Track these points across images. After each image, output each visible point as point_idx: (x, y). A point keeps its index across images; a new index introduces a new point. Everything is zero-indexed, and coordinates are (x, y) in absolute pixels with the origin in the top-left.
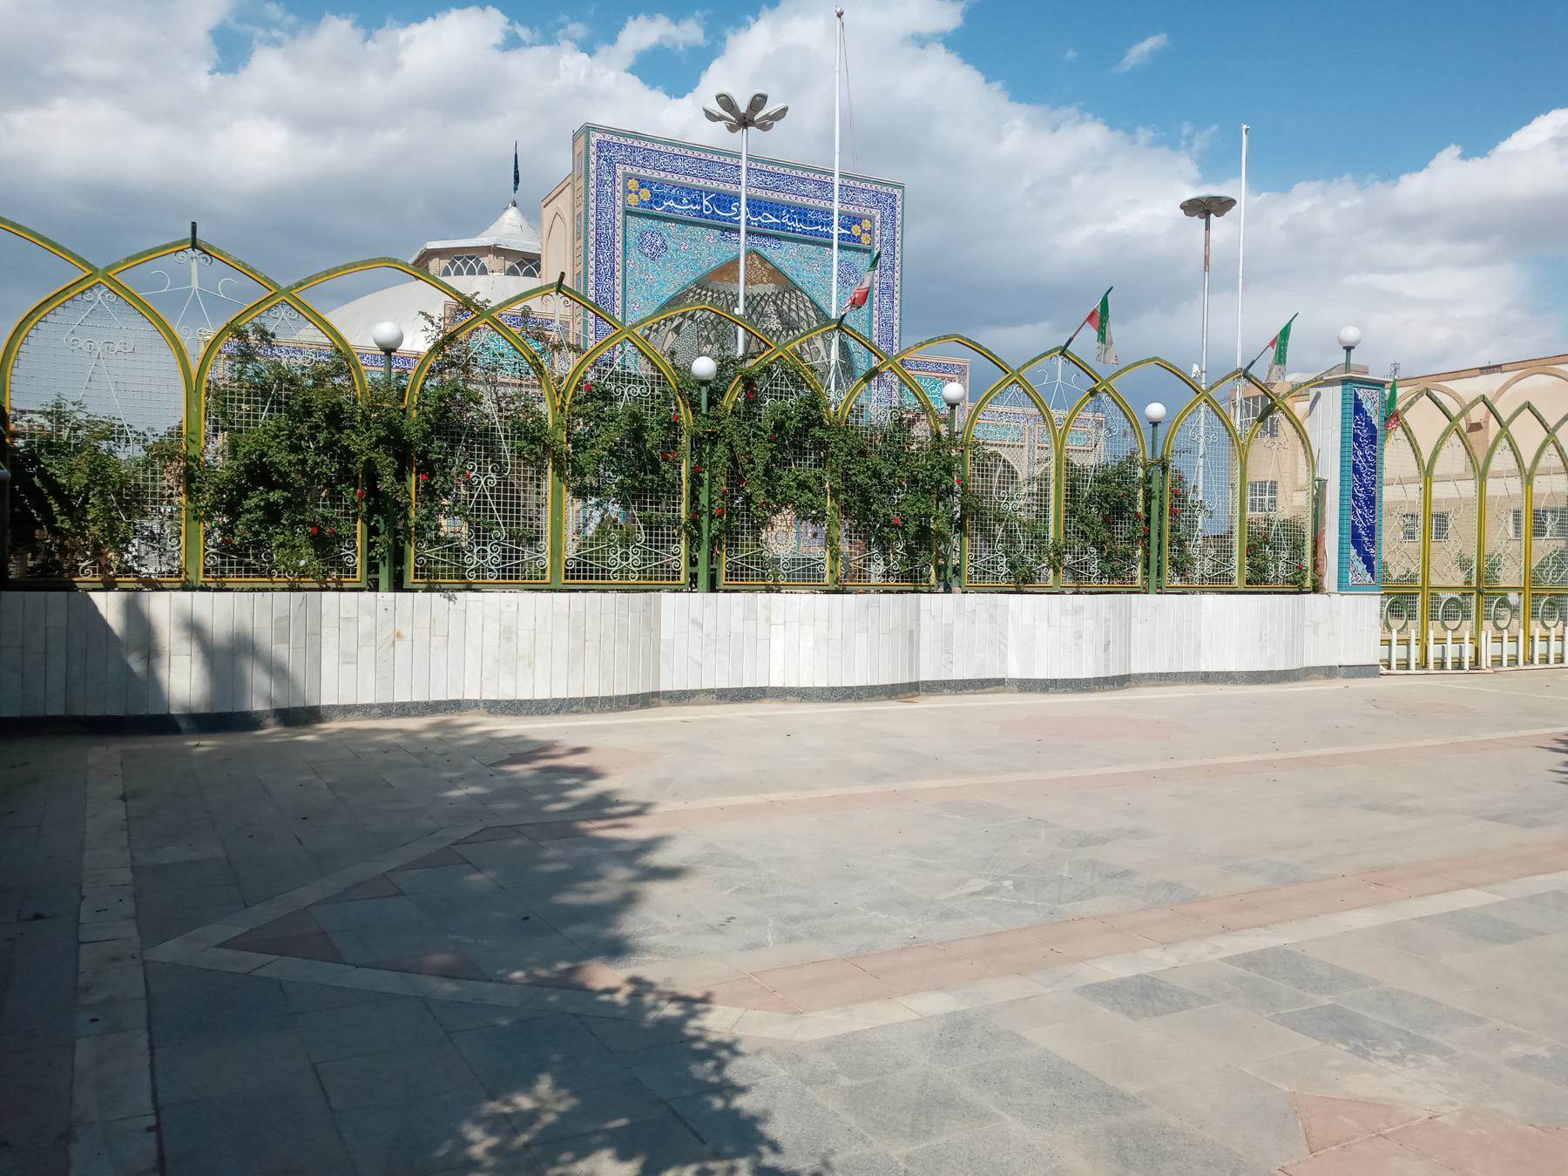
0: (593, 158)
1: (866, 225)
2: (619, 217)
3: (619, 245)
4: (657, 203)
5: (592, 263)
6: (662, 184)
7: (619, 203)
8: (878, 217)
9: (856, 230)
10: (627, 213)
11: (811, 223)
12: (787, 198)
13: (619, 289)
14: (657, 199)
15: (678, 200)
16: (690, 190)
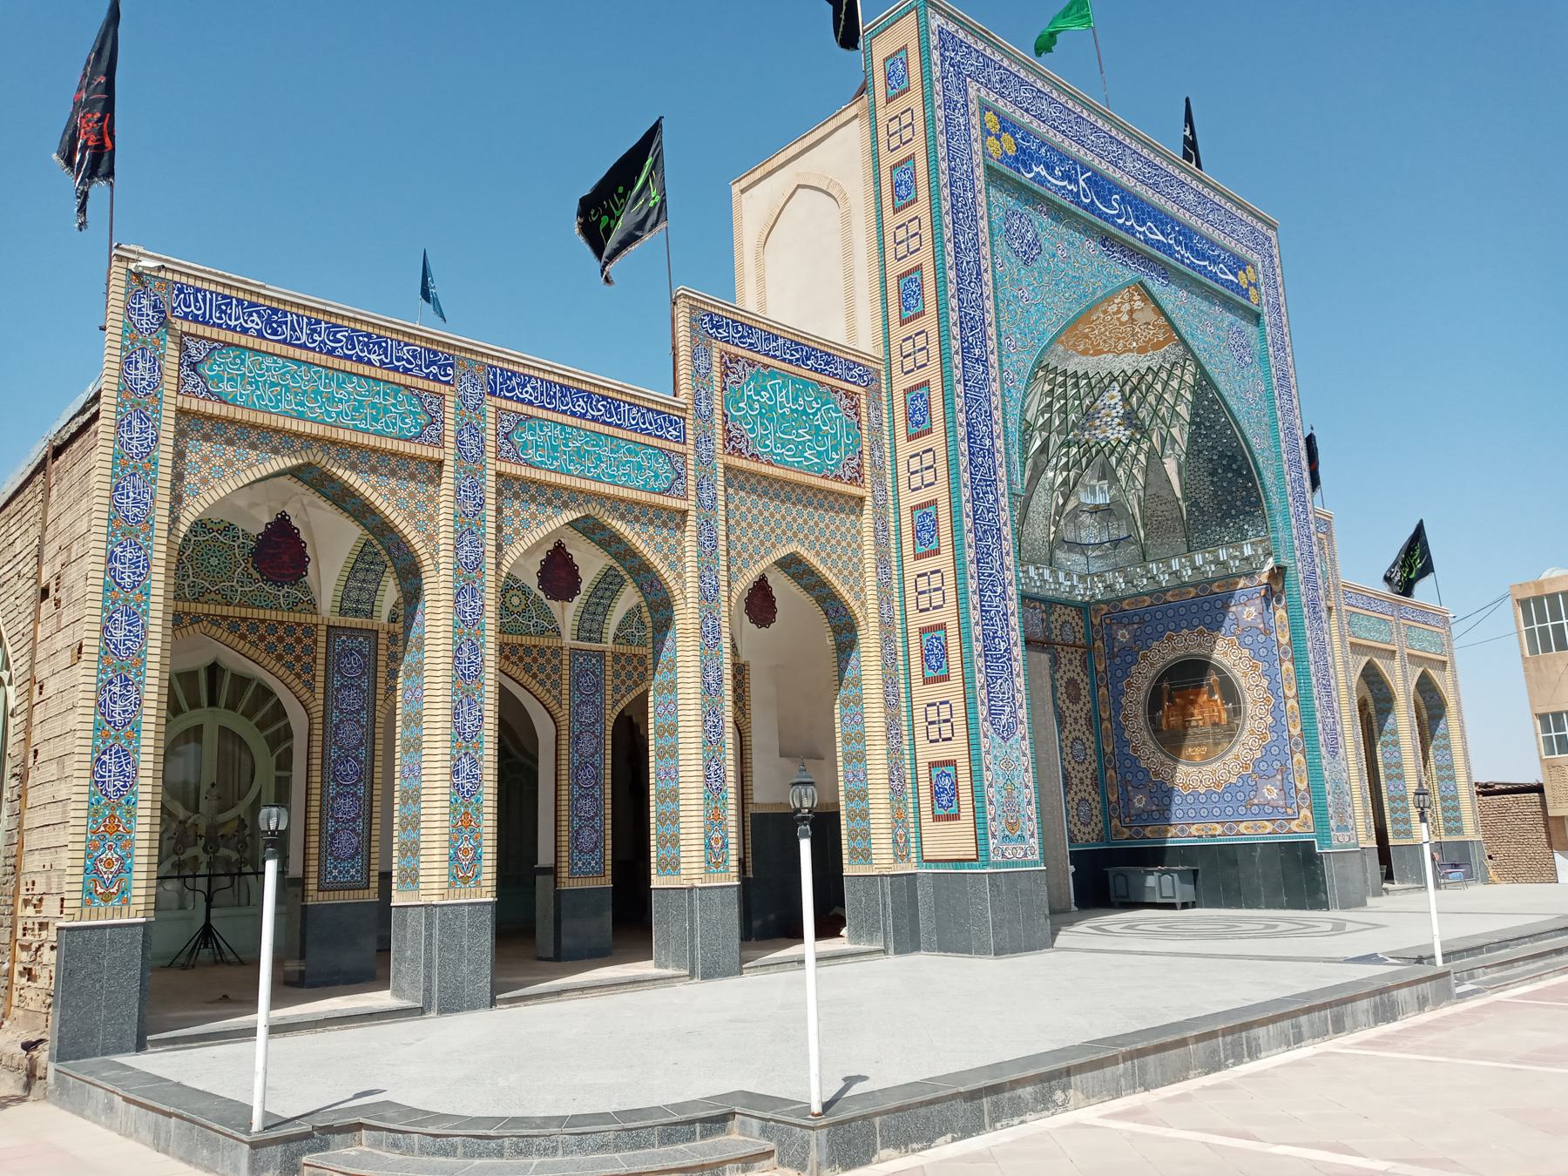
14: (1024, 158)
15: (1050, 168)
16: (1064, 157)
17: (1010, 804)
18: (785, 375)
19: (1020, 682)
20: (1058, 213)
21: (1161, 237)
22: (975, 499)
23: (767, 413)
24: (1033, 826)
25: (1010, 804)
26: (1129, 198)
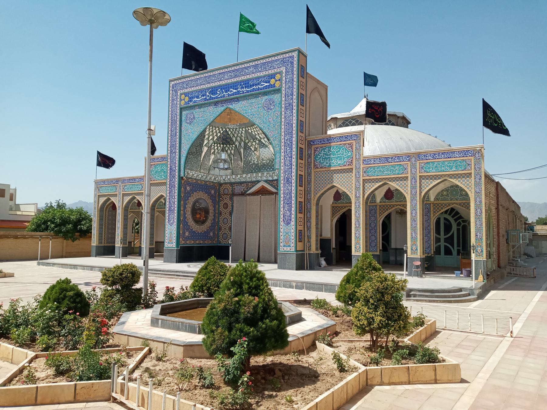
0: (171, 92)
1: (278, 77)
2: (178, 111)
3: (178, 123)
4: (191, 101)
5: (170, 132)
6: (192, 92)
7: (178, 106)
8: (284, 71)
9: (272, 81)
10: (181, 109)
11: (251, 86)
12: (240, 79)
13: (178, 140)
15: (198, 97)
16: (201, 91)
17: (171, 237)
18: (159, 164)
19: (176, 215)
20: (200, 106)
21: (235, 91)
22: (170, 181)
23: (156, 172)
24: (175, 241)
25: (171, 237)
26: (222, 87)
